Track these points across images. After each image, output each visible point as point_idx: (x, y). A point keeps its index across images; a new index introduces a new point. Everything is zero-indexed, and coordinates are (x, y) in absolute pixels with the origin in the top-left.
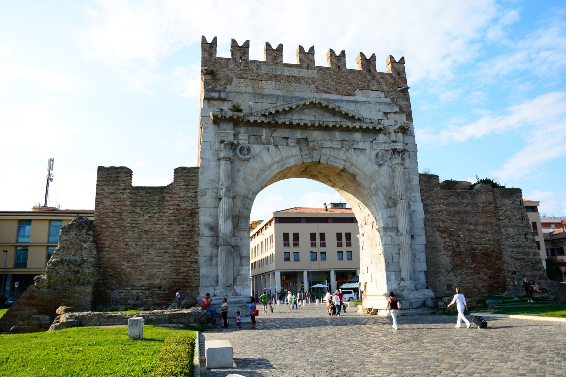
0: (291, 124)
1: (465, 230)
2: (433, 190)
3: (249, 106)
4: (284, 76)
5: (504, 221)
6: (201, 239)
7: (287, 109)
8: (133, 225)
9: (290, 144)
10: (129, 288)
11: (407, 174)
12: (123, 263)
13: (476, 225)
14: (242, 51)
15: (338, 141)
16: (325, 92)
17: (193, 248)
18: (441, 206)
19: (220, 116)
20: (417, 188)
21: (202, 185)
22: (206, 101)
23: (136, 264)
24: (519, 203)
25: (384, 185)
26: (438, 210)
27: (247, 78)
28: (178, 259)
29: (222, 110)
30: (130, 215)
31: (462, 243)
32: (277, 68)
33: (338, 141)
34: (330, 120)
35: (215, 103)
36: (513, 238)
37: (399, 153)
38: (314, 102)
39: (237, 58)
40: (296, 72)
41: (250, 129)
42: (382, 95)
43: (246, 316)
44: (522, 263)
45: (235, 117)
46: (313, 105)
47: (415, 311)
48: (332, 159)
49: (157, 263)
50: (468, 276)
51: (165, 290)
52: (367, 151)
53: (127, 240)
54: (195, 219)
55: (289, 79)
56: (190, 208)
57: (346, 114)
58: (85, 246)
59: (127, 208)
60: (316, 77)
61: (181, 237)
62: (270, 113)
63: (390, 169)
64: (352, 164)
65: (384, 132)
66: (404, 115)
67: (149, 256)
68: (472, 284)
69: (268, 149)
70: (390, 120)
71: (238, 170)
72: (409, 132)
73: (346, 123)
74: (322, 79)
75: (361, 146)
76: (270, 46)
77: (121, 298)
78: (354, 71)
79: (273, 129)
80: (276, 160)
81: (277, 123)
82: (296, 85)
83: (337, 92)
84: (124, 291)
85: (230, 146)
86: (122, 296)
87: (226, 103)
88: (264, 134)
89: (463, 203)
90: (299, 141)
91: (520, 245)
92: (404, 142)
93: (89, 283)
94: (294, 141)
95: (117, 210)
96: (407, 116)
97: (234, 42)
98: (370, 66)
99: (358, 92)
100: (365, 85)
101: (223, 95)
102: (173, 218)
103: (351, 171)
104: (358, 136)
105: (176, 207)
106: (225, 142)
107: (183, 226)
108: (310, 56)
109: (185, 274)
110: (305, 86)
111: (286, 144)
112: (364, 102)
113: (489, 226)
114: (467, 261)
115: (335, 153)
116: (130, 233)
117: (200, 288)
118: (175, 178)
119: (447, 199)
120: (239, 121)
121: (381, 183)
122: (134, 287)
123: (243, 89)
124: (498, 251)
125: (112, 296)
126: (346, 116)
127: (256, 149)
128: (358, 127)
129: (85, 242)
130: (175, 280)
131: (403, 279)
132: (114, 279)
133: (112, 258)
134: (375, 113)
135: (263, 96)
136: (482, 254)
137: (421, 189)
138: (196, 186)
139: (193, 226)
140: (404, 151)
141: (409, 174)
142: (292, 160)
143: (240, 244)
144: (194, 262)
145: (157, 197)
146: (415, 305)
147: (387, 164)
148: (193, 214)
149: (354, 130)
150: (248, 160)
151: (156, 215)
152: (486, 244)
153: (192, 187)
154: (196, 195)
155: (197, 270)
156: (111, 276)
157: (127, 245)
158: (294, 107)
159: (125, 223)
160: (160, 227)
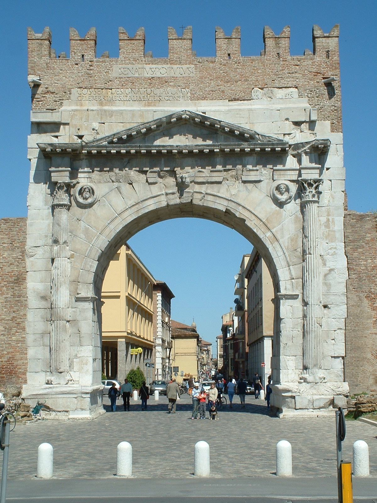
0: (149, 152)
2: (363, 238)
3: (93, 129)
4: (146, 79)
9: (150, 181)
11: (326, 214)
16: (204, 98)
19: (49, 149)
20: (340, 236)
21: (30, 243)
26: (369, 269)
27: (91, 88)
32: (134, 67)
38: (183, 116)
41: (94, 162)
43: (82, 409)
47: (316, 413)
48: (210, 198)
57: (232, 132)
60: (191, 75)
62: (120, 140)
64: (240, 205)
66: (328, 123)
75: (253, 176)
83: (221, 96)
85: (65, 188)
87: (62, 127)
103: (237, 215)
107: (7, 296)
109: (10, 356)
117: (28, 374)
138: (23, 243)
139: (19, 296)
141: (328, 215)
142: (151, 202)
146: (317, 404)
150: (91, 205)
155: (24, 351)
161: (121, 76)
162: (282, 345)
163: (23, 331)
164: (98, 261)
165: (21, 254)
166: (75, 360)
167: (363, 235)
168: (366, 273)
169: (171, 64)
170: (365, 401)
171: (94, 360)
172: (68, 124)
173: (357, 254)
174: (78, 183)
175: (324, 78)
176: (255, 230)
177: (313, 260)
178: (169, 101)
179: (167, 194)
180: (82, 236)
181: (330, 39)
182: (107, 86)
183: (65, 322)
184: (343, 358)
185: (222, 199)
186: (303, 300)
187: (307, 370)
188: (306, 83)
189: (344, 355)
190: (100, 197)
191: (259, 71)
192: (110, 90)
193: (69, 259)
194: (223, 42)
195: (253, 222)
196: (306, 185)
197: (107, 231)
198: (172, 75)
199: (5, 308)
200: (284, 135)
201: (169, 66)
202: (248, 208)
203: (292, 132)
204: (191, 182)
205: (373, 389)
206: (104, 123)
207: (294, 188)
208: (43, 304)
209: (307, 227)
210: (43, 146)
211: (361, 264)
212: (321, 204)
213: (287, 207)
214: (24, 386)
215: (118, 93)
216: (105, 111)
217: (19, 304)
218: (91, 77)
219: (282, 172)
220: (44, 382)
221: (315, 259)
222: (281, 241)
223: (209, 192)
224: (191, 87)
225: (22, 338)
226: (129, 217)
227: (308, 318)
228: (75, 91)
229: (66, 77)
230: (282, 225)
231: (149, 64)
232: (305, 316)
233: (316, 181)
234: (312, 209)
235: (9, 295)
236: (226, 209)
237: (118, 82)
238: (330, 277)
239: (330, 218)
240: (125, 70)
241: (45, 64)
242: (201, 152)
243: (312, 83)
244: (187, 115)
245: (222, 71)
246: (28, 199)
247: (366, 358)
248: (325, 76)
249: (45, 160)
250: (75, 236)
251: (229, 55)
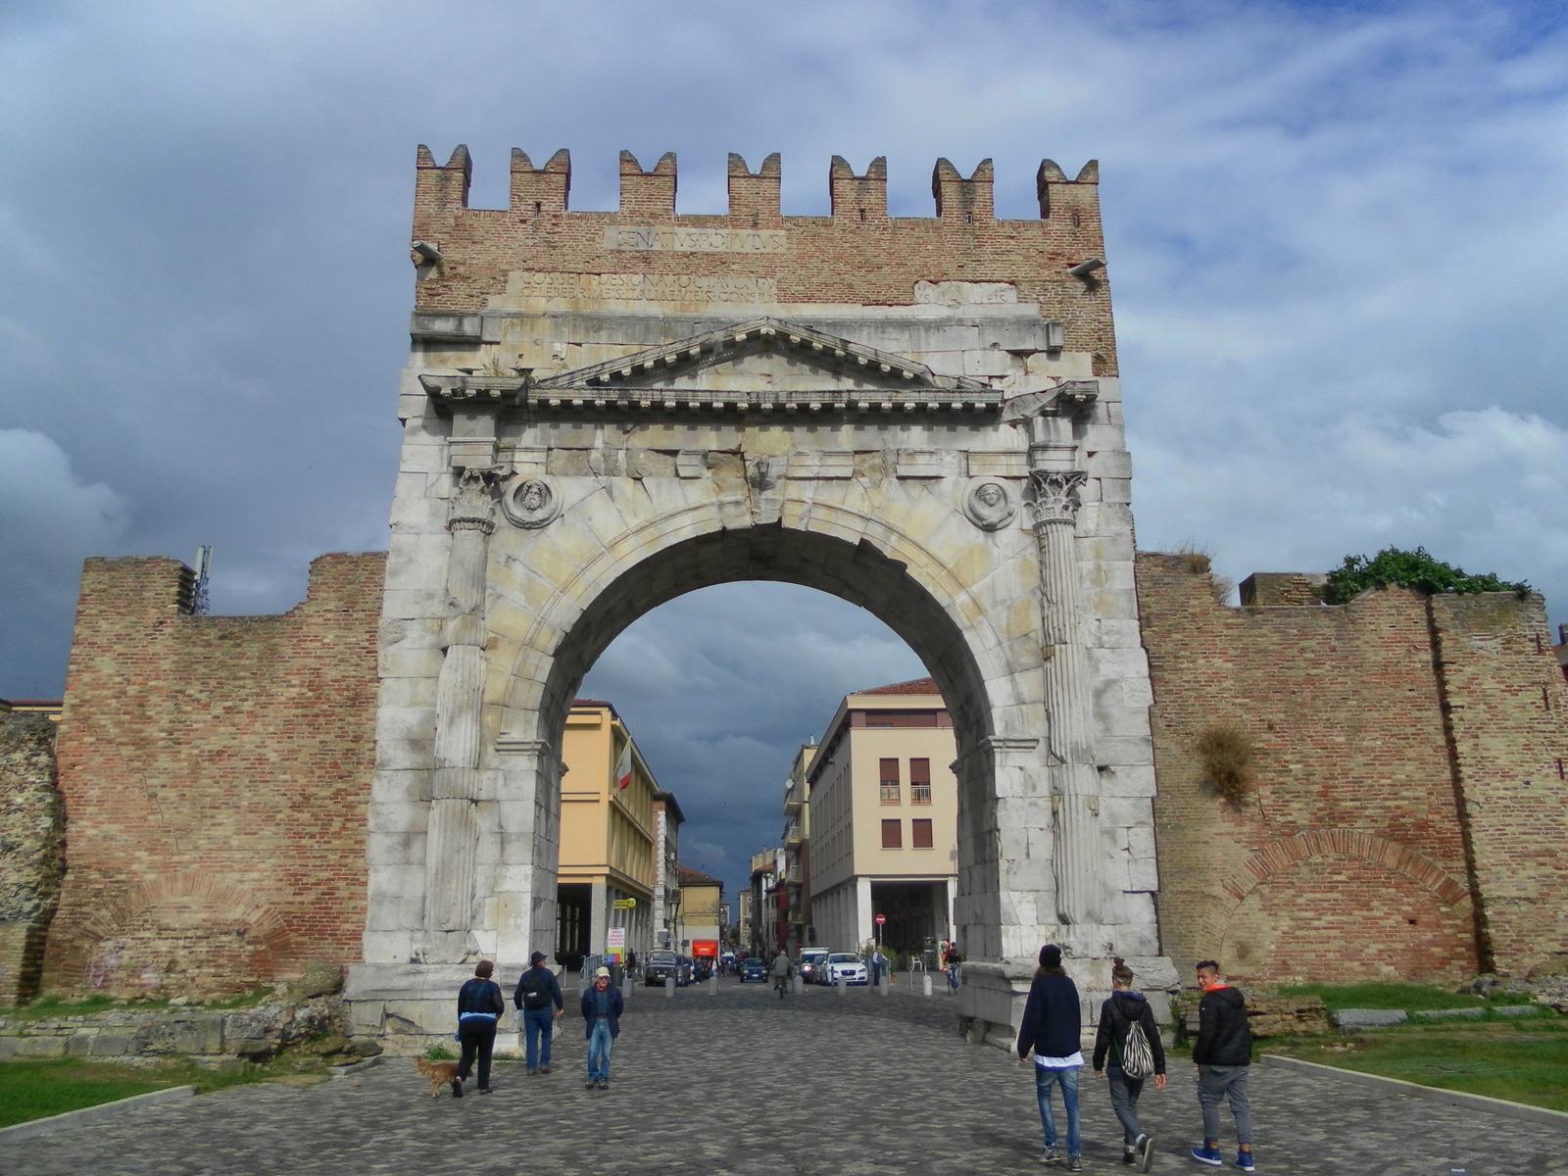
0: (682, 406)
1: (1308, 748)
2: (1184, 607)
4: (675, 255)
5: (1468, 715)
6: (379, 777)
7: (670, 359)
8: (176, 735)
10: (147, 934)
12: (138, 854)
13: (1356, 729)
14: (543, 186)
15: (844, 453)
16: (809, 299)
17: (350, 806)
18: (1218, 662)
19: (446, 391)
21: (393, 608)
22: (420, 346)
23: (176, 858)
24: (1530, 647)
25: (1002, 594)
26: (1202, 678)
27: (554, 270)
28: (304, 842)
29: (469, 372)
30: (169, 705)
31: (1297, 795)
33: (844, 453)
34: (814, 386)
35: (449, 354)
36: (1505, 775)
37: (1055, 483)
38: (763, 331)
39: (526, 209)
40: (714, 241)
42: (1011, 295)
44: (1548, 870)
45: (495, 393)
46: (761, 344)
48: (821, 513)
49: (237, 856)
50: (1321, 914)
51: (254, 941)
52: (945, 485)
53: (156, 782)
54: (365, 716)
55: (689, 260)
56: (352, 682)
58: (19, 800)
59: (161, 683)
60: (781, 250)
61: (318, 772)
62: (617, 377)
63: (1028, 540)
64: (890, 529)
65: (1007, 415)
66: (1086, 360)
67: (218, 832)
68: (1335, 944)
69: (609, 490)
70: (1031, 377)
72: (1101, 410)
73: (868, 394)
74: (801, 256)
76: (633, 161)
77: (120, 967)
78: (914, 223)
79: (629, 427)
80: (634, 523)
81: (634, 406)
82: (713, 280)
83: (848, 295)
84: (131, 943)
85: (482, 483)
86: (125, 960)
88: (599, 443)
89: (1303, 650)
90: (709, 460)
91: (1538, 800)
92: (1074, 448)
93: (18, 914)
94: (696, 460)
95: (132, 690)
97: (519, 155)
98: (972, 201)
99: (924, 291)
100: (950, 267)
101: (469, 328)
102: (299, 711)
103: (889, 554)
104: (916, 436)
105: (308, 677)
106: (467, 474)
108: (766, 184)
109: (323, 888)
110: (742, 281)
111: (670, 471)
112: (939, 325)
113: (1409, 730)
114: (1317, 859)
115: (832, 495)
116: (164, 761)
117: (365, 935)
118: (312, 589)
119: (1239, 638)
120: (514, 407)
121: (992, 588)
122: (161, 930)
123: (540, 304)
124: (1447, 825)
125: (95, 958)
126: (872, 371)
127: (568, 490)
128: (910, 405)
129: (21, 789)
130: (292, 909)
131: (1064, 920)
132: (105, 905)
133: (106, 838)
134: (978, 355)
135: (597, 323)
136: (1379, 834)
138: (377, 612)
139: (357, 739)
140: (1076, 477)
141: (1098, 556)
143: (501, 794)
144: (352, 851)
145: (253, 649)
147: (1015, 525)
148: (361, 699)
149: (899, 416)
150: (541, 525)
151: (247, 706)
152: (1396, 796)
153: (361, 615)
154: (372, 640)
155: (358, 880)
156: (98, 893)
157: (154, 796)
159: (152, 731)
160: (257, 739)
161: (623, 248)
162: (1003, 865)
163: (360, 825)
164: (553, 656)
165: (367, 636)
166: (487, 901)
167: (1183, 603)
168: (1194, 689)
169: (734, 227)
170: (1262, 1008)
171: (536, 902)
172: (498, 343)
173: (1170, 644)
174: (514, 473)
175: (1071, 265)
176: (930, 589)
177: (1071, 658)
178: (729, 303)
179: (721, 505)
180: (519, 597)
181: (1080, 186)
182: (589, 267)
183: (465, 802)
184: (1152, 893)
185: (851, 517)
186: (1051, 752)
187: (1071, 926)
188: (1032, 274)
189: (1155, 888)
190: (566, 507)
191: (929, 247)
192: (596, 277)
193: (483, 649)
194: (849, 187)
195: (925, 569)
196: (1045, 486)
197: (579, 588)
198: (737, 248)
199: (320, 768)
200: (990, 377)
201: (730, 230)
202: (912, 538)
203: (1008, 373)
204: (779, 477)
205: (1232, 974)
206: (580, 345)
207: (1015, 491)
208: (418, 759)
209: (1053, 580)
210: (432, 382)
211: (1182, 669)
212: (1081, 530)
213: (1002, 536)
214: (352, 968)
215: (614, 282)
216: (582, 316)
217: (355, 758)
218: (554, 248)
219: (989, 459)
220: (406, 959)
221: (1075, 655)
222: (991, 612)
223: (820, 499)
224: (778, 276)
225: (356, 842)
226: (632, 555)
227: (1067, 798)
228: (516, 278)
229: (498, 247)
230: (993, 578)
231: (686, 225)
232: (1056, 793)
233: (1068, 476)
234: (1061, 538)
235: (332, 736)
236: (863, 541)
237: (616, 260)
238: (1108, 699)
239: (1102, 563)
240: (632, 235)
241: (453, 220)
242: (804, 408)
243: (1046, 273)
244: (772, 327)
245: (846, 245)
246: (394, 509)
247: (1210, 896)
248: (1073, 262)
249: (437, 421)
250: (499, 596)
251: (862, 211)
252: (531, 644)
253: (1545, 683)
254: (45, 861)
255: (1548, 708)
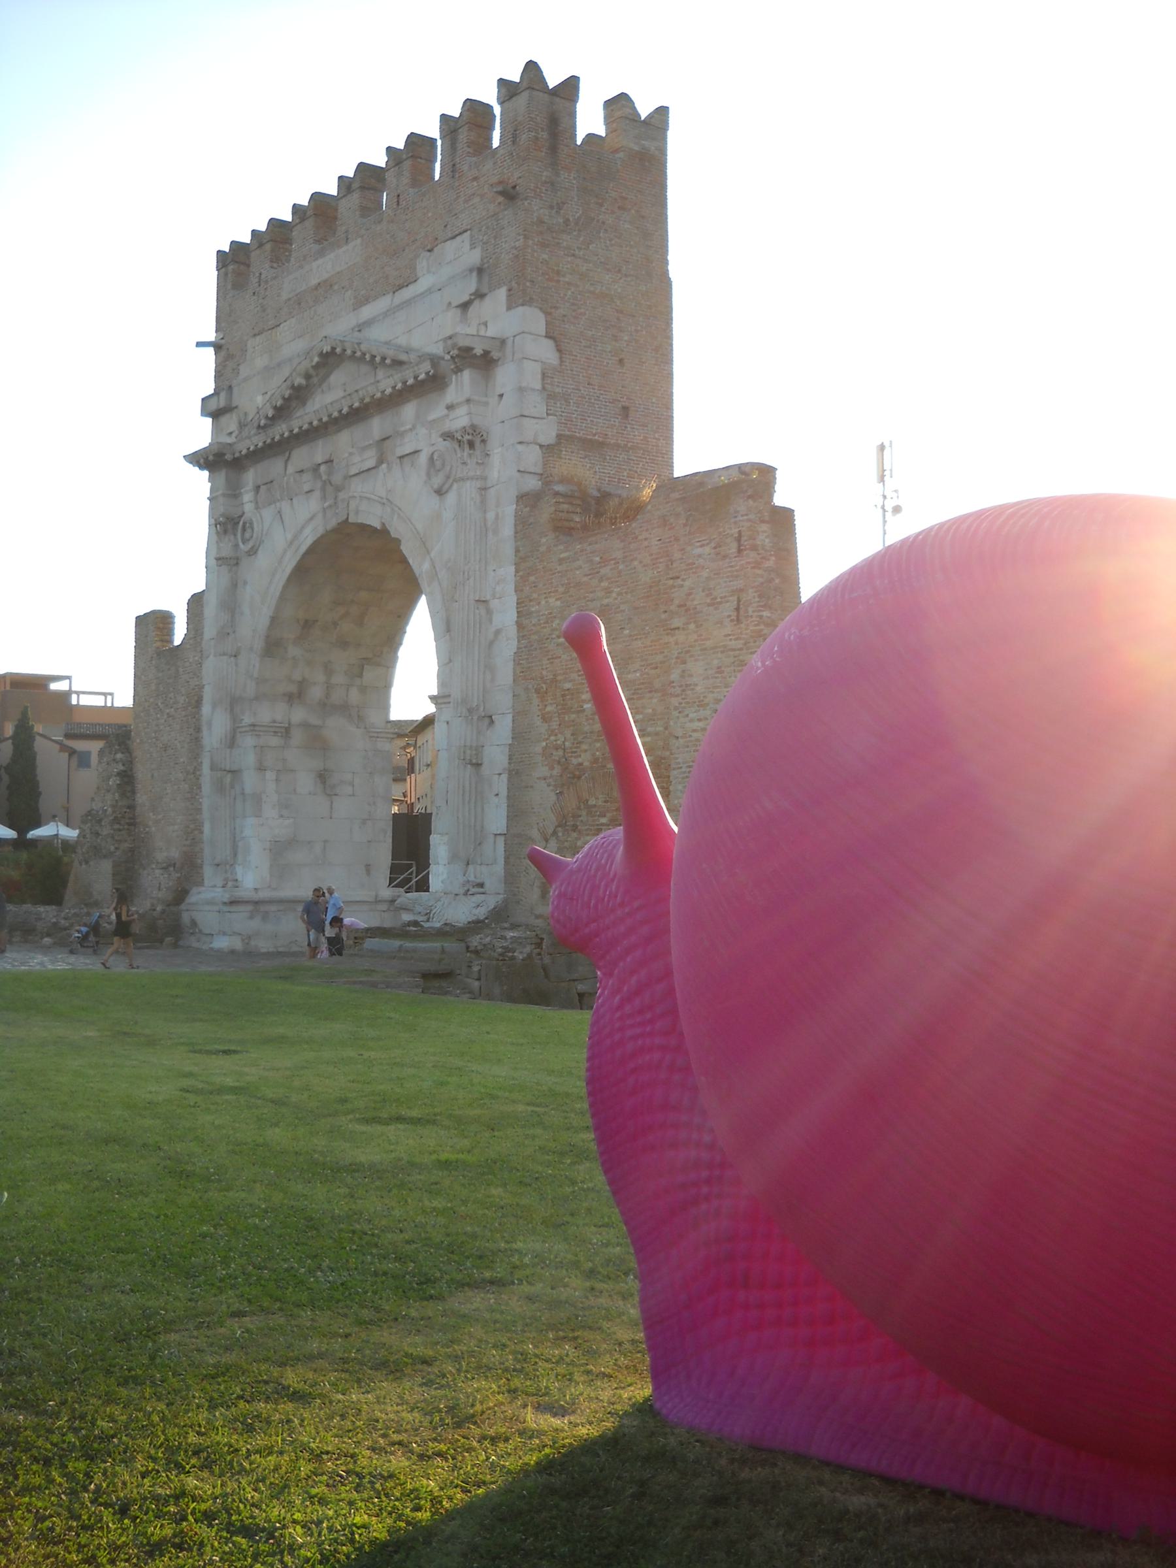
36: (702, 705)
46: (330, 359)
71: (245, 583)
96: (510, 290)
104: (409, 411)
137: (517, 551)
158: (299, 381)
252: (251, 649)
253: (741, 590)
254: (116, 820)
255: (738, 620)
